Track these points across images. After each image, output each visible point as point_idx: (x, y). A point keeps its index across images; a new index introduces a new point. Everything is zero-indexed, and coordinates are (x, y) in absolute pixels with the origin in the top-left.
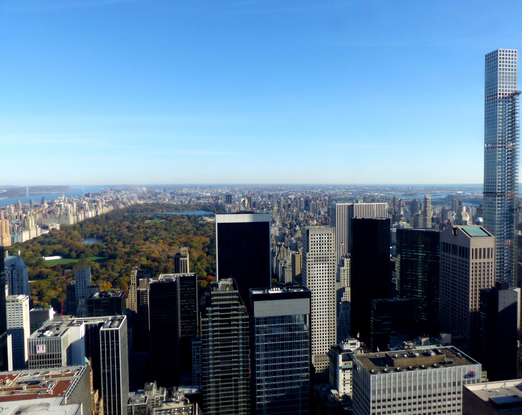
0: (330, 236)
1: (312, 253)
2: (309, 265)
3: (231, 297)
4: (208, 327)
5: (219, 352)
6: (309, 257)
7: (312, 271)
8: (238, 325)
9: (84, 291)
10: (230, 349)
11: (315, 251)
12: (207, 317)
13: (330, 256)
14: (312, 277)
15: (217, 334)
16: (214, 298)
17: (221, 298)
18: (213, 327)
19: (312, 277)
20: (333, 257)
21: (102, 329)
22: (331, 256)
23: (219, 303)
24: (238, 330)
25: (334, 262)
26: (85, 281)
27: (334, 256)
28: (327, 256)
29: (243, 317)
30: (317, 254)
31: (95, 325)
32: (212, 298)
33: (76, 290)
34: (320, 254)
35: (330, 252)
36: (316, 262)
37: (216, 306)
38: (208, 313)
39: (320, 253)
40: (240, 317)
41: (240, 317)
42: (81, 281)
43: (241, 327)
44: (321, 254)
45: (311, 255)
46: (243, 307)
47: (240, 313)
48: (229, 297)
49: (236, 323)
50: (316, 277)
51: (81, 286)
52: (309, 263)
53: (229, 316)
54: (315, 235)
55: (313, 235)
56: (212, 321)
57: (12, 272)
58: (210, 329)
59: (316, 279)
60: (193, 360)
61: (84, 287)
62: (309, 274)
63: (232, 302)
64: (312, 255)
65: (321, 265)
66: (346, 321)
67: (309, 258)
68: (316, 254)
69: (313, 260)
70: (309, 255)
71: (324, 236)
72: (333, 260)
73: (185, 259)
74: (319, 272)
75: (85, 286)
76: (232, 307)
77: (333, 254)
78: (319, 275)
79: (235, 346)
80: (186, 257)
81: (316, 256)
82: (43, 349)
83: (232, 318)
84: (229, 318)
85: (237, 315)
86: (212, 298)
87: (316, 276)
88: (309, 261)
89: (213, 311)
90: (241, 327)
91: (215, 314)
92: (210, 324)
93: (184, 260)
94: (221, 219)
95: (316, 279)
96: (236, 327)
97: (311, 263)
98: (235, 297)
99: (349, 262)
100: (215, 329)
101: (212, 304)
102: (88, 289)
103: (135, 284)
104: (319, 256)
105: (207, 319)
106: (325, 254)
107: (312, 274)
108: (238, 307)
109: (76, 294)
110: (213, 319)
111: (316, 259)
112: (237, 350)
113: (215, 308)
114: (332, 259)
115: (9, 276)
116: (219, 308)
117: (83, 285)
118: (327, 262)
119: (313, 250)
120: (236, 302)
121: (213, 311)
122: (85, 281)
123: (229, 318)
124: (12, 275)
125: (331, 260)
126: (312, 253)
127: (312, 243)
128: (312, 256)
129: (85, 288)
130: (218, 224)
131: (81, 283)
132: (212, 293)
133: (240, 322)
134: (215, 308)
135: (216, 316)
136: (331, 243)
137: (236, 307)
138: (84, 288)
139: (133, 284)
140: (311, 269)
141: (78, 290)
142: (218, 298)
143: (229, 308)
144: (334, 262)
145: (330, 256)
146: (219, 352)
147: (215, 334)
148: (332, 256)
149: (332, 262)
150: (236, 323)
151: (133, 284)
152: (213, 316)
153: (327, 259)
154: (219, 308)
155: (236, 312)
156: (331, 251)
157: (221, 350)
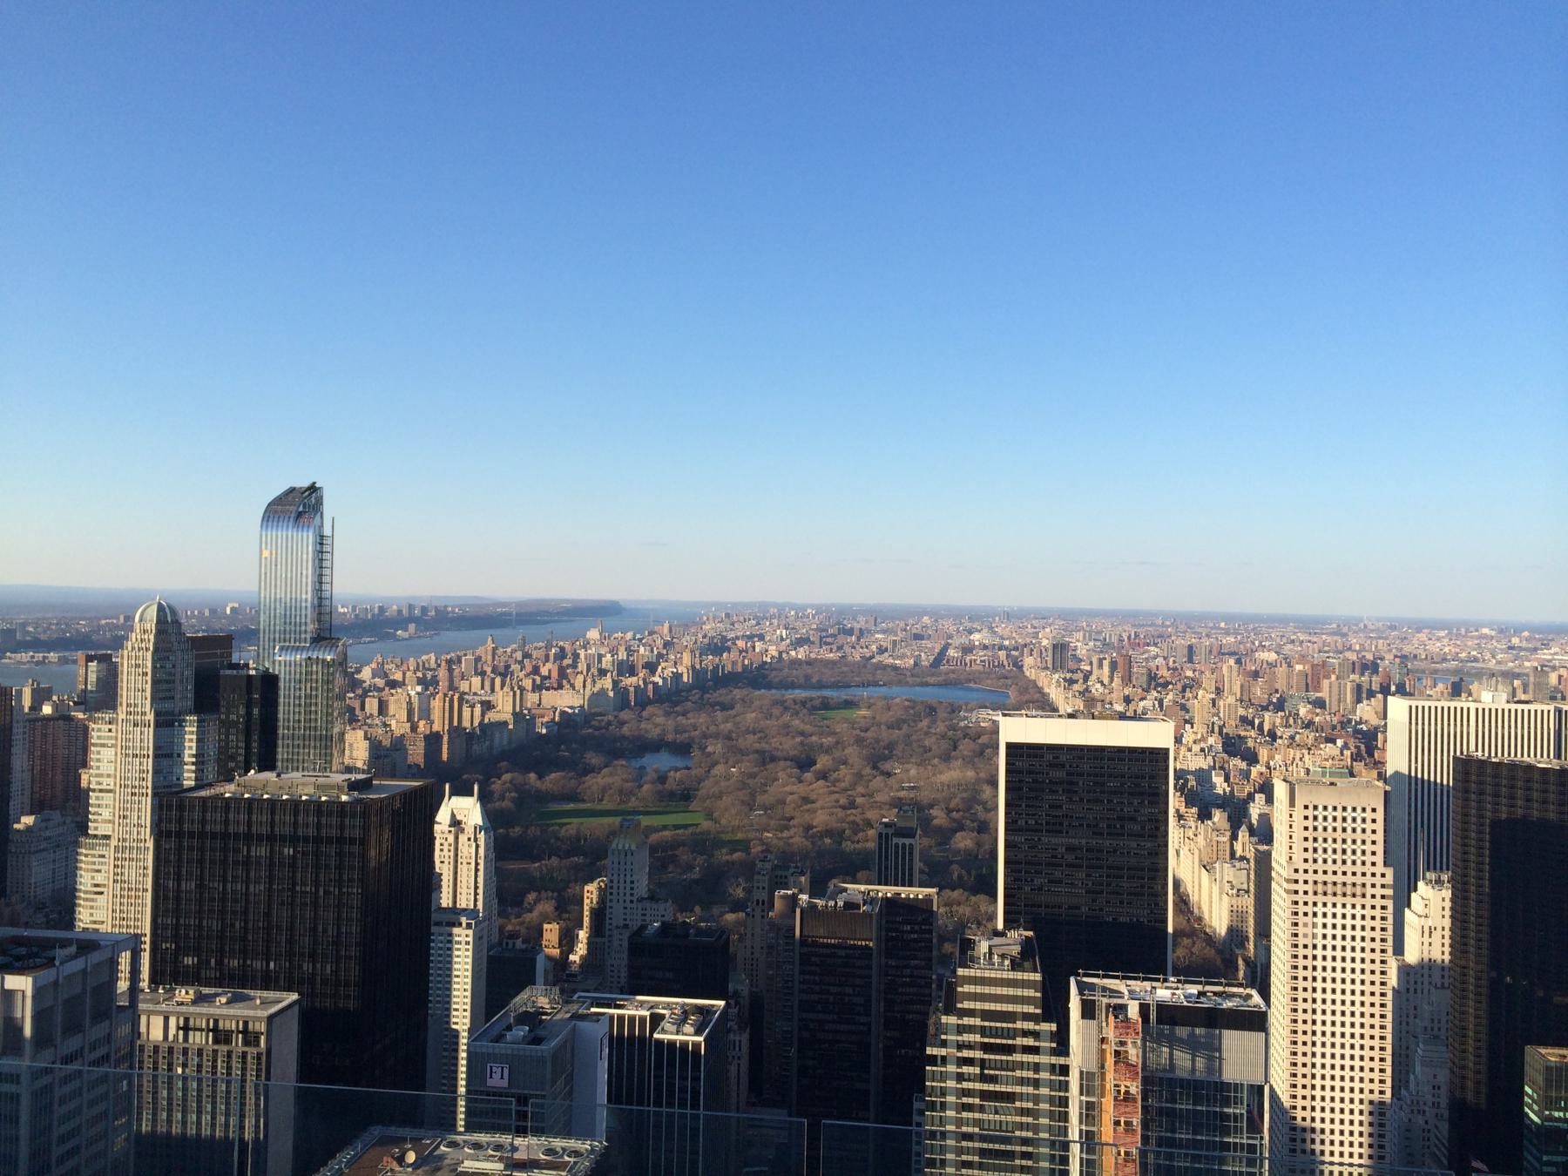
0: (1369, 815)
1: (1306, 866)
2: (1296, 903)
3: (1019, 992)
4: (943, 1077)
5: (976, 1159)
6: (1296, 876)
7: (1305, 925)
8: (1036, 1083)
9: (628, 911)
10: (1010, 1155)
11: (1315, 861)
12: (944, 1044)
13: (1368, 880)
14: (1305, 946)
15: (970, 1100)
16: (967, 988)
17: (987, 990)
18: (960, 1077)
19: (1305, 946)
20: (1383, 886)
21: (656, 1036)
22: (1373, 880)
23: (978, 1006)
24: (1036, 1099)
25: (1384, 902)
26: (632, 882)
27: (1384, 881)
28: (1359, 880)
29: (1054, 1060)
30: (1325, 872)
31: (643, 1019)
32: (959, 989)
33: (608, 904)
34: (1335, 873)
35: (1369, 869)
36: (1320, 899)
37: (971, 1013)
38: (946, 1034)
39: (1335, 868)
40: (1044, 1059)
41: (1044, 1059)
42: (622, 881)
43: (1044, 1091)
44: (1340, 873)
45: (1301, 871)
46: (1054, 1027)
47: (1042, 1044)
48: (1011, 991)
49: (1031, 1074)
50: (1320, 947)
51: (622, 895)
52: (1295, 897)
53: (1010, 1050)
54: (1315, 808)
55: (1311, 807)
56: (958, 1058)
57: (457, 838)
58: (951, 1084)
59: (1319, 952)
60: (914, 1158)
61: (628, 898)
62: (1296, 935)
63: (1019, 1008)
64: (1306, 871)
65: (1339, 910)
66: (1436, 1105)
67: (1296, 882)
68: (1320, 872)
69: (1309, 888)
70: (1296, 871)
71: (1349, 814)
72: (1383, 897)
73: (907, 841)
74: (1329, 931)
75: (632, 895)
76: (1019, 1025)
77: (1383, 875)
78: (1329, 942)
79: (1024, 1149)
80: (913, 836)
81: (1320, 877)
82: (502, 1078)
83: (1017, 1057)
84: (1010, 1058)
85: (1035, 1050)
86: (959, 989)
87: (1320, 942)
88: (1296, 892)
89: (961, 1029)
90: (1044, 1091)
91: (966, 1037)
92: (951, 1068)
93: (904, 845)
94: (1018, 729)
95: (1319, 952)
96: (1030, 1090)
97: (1301, 898)
98: (1031, 993)
99: (1448, 904)
100: (965, 1085)
101: (959, 1006)
102: (640, 905)
103: (763, 901)
104: (1330, 878)
105: (943, 1052)
106: (1354, 874)
107: (1305, 936)
108: (1037, 1027)
109: (608, 916)
110: (959, 1055)
111: (1320, 888)
112: (1030, 1163)
113: (966, 1021)
114: (1379, 891)
115: (449, 851)
116: (978, 1022)
117: (628, 891)
118: (1358, 901)
119: (1309, 855)
120: (1031, 1009)
121: (961, 1029)
122: (632, 882)
123: (1010, 1058)
124: (456, 849)
125: (1373, 896)
126: (1306, 866)
127: (1306, 834)
128: (1306, 877)
129: (632, 902)
130: (1009, 746)
131: (622, 885)
132: (961, 972)
133: (1044, 1075)
134: (966, 1021)
135: (970, 1046)
136: (1374, 837)
137: (1030, 1026)
138: (628, 901)
139: (758, 901)
140: (1301, 919)
141: (614, 904)
142: (979, 989)
143: (1010, 1025)
144: (1384, 902)
145: (1368, 880)
146: (976, 1159)
147: (965, 1100)
148: (1378, 880)
149: (1378, 902)
150: (1031, 1074)
151: (758, 901)
152: (960, 1046)
153: (1359, 890)
154: (978, 1022)
155: (1030, 1042)
156: (1373, 864)
157: (983, 1153)
